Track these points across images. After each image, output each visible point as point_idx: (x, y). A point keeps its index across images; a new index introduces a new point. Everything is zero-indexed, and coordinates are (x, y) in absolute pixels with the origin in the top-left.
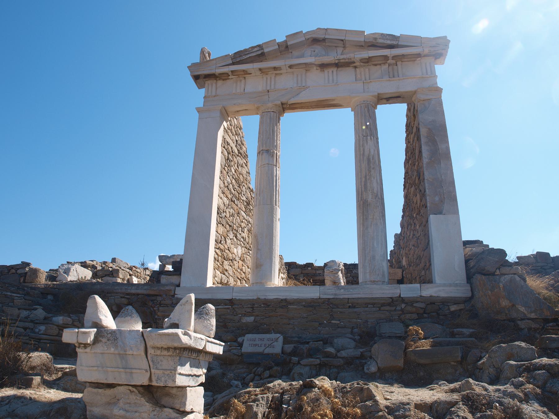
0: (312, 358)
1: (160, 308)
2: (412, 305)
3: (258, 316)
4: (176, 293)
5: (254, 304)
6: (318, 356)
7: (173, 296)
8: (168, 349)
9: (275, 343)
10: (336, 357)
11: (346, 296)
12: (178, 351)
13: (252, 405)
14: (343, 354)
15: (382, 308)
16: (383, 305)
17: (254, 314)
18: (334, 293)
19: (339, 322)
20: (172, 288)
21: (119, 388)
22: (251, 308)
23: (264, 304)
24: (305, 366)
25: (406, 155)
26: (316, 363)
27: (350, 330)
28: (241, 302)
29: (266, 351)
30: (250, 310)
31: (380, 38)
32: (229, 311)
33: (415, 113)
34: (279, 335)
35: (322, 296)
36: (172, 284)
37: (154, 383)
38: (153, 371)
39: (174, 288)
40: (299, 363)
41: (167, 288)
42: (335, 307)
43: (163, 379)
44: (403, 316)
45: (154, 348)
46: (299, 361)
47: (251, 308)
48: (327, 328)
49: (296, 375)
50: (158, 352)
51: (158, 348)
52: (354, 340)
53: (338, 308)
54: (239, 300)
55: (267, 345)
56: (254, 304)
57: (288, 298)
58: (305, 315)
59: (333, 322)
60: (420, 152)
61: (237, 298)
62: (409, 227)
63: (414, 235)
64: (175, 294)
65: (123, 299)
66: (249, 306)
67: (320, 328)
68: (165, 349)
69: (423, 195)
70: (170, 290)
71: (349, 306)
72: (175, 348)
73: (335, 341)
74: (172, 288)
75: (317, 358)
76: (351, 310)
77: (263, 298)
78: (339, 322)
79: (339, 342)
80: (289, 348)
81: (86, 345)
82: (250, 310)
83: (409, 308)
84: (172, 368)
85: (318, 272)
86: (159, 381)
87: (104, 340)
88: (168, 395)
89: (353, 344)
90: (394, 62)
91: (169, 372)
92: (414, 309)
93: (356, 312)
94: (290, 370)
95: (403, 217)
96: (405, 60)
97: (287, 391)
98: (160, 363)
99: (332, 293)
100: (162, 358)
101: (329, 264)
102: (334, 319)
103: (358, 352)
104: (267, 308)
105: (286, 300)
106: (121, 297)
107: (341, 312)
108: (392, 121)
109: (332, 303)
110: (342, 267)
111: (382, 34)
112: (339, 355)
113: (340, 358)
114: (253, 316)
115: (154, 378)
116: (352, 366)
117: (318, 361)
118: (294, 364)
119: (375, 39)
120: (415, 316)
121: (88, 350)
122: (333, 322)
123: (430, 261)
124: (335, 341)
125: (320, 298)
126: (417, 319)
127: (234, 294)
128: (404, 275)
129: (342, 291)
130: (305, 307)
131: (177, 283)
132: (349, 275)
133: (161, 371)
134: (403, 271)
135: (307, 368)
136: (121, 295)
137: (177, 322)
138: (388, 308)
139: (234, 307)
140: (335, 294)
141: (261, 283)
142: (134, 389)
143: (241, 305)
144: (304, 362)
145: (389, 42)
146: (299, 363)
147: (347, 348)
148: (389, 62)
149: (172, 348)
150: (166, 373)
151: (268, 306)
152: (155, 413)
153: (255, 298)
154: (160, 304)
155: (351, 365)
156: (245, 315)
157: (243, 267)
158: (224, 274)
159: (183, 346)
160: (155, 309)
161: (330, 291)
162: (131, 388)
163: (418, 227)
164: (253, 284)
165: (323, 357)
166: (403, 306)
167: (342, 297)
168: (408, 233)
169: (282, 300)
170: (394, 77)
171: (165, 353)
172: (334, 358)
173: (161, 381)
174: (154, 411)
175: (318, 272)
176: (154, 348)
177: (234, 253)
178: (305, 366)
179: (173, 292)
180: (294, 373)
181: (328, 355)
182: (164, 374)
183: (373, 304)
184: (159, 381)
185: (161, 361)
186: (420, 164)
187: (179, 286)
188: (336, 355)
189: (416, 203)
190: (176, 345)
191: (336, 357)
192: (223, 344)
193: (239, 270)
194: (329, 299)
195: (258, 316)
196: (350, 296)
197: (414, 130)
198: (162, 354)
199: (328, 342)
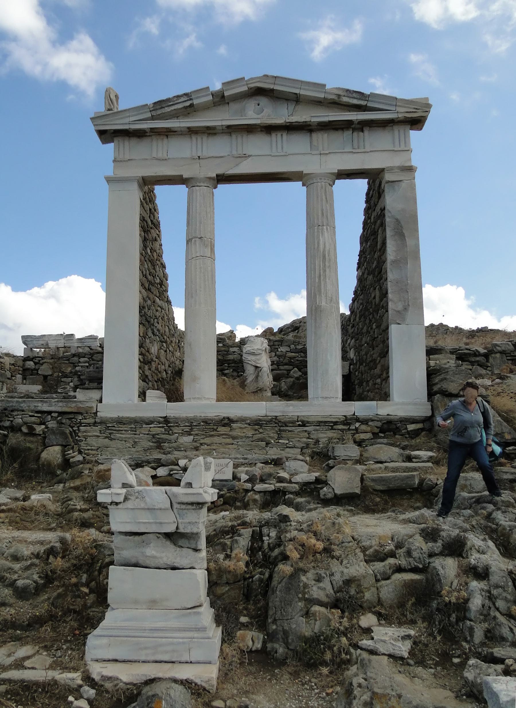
0: (266, 483)
1: (81, 428)
2: (367, 424)
6: (271, 482)
7: (96, 414)
9: (225, 469)
11: (297, 414)
14: (298, 478)
15: (335, 427)
16: (336, 423)
19: (288, 442)
21: (149, 535)
23: (203, 422)
25: (364, 228)
26: (271, 489)
30: (187, 429)
31: (344, 96)
33: (381, 191)
37: (181, 530)
38: (180, 521)
41: (88, 405)
44: (357, 435)
45: (179, 503)
46: (252, 487)
50: (183, 507)
51: (183, 503)
52: (306, 462)
53: (287, 426)
55: (217, 471)
59: (280, 441)
60: (384, 243)
62: (362, 319)
63: (368, 332)
64: (97, 412)
65: (33, 418)
66: (187, 424)
69: (384, 294)
75: (271, 484)
78: (288, 442)
81: (117, 504)
83: (364, 427)
85: (232, 350)
87: (132, 498)
89: (307, 467)
90: (359, 126)
92: (369, 429)
93: (306, 431)
95: (354, 300)
96: (374, 125)
103: (312, 477)
106: (31, 416)
107: (290, 431)
108: (351, 196)
111: (347, 90)
112: (293, 480)
113: (295, 483)
115: (180, 526)
119: (339, 96)
120: (369, 436)
121: (120, 506)
122: (280, 441)
123: (388, 373)
126: (372, 439)
127: (168, 411)
128: (351, 370)
129: (291, 408)
130: (249, 425)
131: (98, 397)
134: (350, 365)
136: (31, 414)
138: (341, 427)
140: (283, 412)
142: (160, 535)
143: (177, 423)
145: (355, 102)
148: (353, 126)
152: (177, 552)
154: (81, 423)
160: (74, 428)
162: (157, 535)
163: (374, 327)
166: (357, 425)
168: (360, 324)
170: (358, 148)
171: (190, 507)
174: (176, 551)
175: (232, 350)
176: (179, 503)
177: (152, 353)
181: (281, 480)
183: (326, 422)
186: (383, 258)
187: (101, 401)
188: (290, 480)
189: (375, 298)
191: (290, 482)
193: (156, 371)
194: (276, 417)
195: (197, 435)
197: (378, 209)
198: (187, 508)
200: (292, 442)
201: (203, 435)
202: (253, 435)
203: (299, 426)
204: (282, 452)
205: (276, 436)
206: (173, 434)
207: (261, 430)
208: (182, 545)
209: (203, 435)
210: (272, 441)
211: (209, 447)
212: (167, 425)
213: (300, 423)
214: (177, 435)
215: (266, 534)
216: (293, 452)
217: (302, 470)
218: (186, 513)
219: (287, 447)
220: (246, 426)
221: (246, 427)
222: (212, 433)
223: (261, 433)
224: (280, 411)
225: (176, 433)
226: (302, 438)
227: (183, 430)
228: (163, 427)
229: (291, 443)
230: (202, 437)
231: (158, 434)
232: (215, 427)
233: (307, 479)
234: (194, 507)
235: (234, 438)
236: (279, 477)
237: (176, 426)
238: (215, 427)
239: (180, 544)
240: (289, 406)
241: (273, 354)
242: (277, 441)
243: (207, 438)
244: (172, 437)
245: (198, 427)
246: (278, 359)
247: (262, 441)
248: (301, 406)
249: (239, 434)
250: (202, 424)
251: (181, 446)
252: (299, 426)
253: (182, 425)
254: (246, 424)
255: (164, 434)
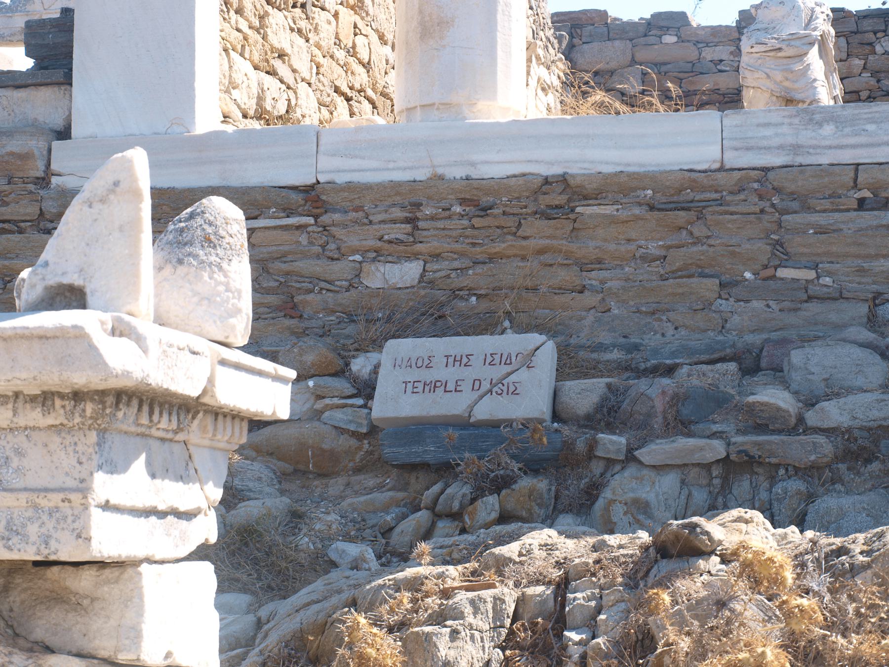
0: (690, 435)
3: (436, 256)
4: (54, 166)
5: (418, 205)
6: (716, 428)
7: (43, 181)
8: (45, 399)
9: (523, 375)
10: (800, 427)
11: (847, 156)
12: (89, 408)
13: (428, 636)
14: (834, 413)
17: (419, 247)
18: (790, 140)
19: (812, 275)
20: (36, 145)
22: (407, 221)
23: (463, 202)
24: (659, 469)
26: (709, 457)
27: (864, 309)
28: (359, 199)
29: (485, 411)
30: (399, 231)
32: (303, 239)
34: (536, 338)
35: (735, 159)
36: (35, 128)
39: (43, 144)
40: (630, 458)
42: (795, 205)
43: (33, 530)
47: (407, 221)
48: (756, 304)
49: (618, 513)
53: (807, 208)
54: (350, 187)
56: (418, 205)
57: (574, 170)
58: (653, 248)
61: (341, 179)
66: (397, 213)
67: (723, 305)
68: (33, 399)
70: (26, 157)
71: (861, 202)
72: (78, 396)
73: (797, 357)
74: (36, 145)
75: (713, 435)
76: (868, 218)
77: (459, 172)
79: (812, 361)
80: (585, 394)
82: (399, 231)
84: (71, 483)
85: (709, 54)
86: (15, 540)
88: (60, 598)
91: (55, 499)
94: (592, 492)
97: (585, 572)
98: (15, 462)
99: (776, 142)
100: (20, 439)
101: (761, 15)
102: (786, 258)
104: (477, 222)
105: (563, 180)
107: (821, 231)
109: (777, 190)
110: (824, 26)
112: (812, 418)
114: (415, 256)
116: (875, 466)
117: (717, 449)
118: (610, 462)
122: (782, 273)
124: (797, 357)
125: (721, 169)
127: (325, 163)
129: (828, 129)
130: (652, 208)
131: (58, 122)
132: (858, 63)
133: (23, 496)
135: (669, 482)
137: (77, 281)
139: (325, 219)
140: (796, 148)
141: (447, 105)
143: (357, 209)
144: (654, 451)
146: (630, 458)
147: (850, 391)
149: (62, 396)
150: (43, 502)
151: (485, 210)
153: (422, 175)
155: (868, 461)
156: (378, 255)
157: (360, 40)
158: (272, 73)
159: (113, 384)
161: (768, 132)
164: (409, 110)
165: (739, 432)
167: (825, 160)
169: (547, 181)
171: (34, 416)
172: (792, 431)
173: (25, 538)
178: (659, 469)
179: (41, 165)
180: (611, 502)
181: (762, 422)
182: (36, 507)
184: (15, 540)
185: (19, 453)
187: (64, 134)
188: (801, 420)
190: (80, 379)
191: (800, 427)
192: (292, 374)
193: (340, 55)
194: (765, 170)
195: (436, 256)
196: (863, 156)
198: (21, 421)
199: (764, 363)
200: (829, 274)
201: (462, 254)
202: (668, 248)
203: (862, 204)
204: (791, 319)
205: (761, 250)
206: (341, 255)
207: (699, 230)
208: (51, 641)
209: (462, 254)
210: (748, 275)
211: (485, 305)
212: (316, 217)
213: (866, 194)
214: (358, 257)
215: (578, 617)
216: (833, 317)
217: (860, 382)
218: (19, 453)
219: (810, 298)
220: (637, 211)
221: (637, 218)
222: (499, 247)
223: (698, 241)
224: (781, 147)
225: (355, 251)
226: (877, 256)
227: (381, 239)
228: (300, 227)
229: (827, 280)
230: (456, 264)
231: (282, 257)
232: (511, 222)
233: (875, 414)
234: (56, 418)
235: (584, 266)
236: (751, 408)
237: (356, 222)
238: (511, 222)
239: (39, 633)
240: (820, 124)
241: (858, 63)
242: (769, 272)
243: (479, 269)
244: (337, 266)
245: (440, 224)
246: (873, 82)
247: (703, 275)
248: (872, 121)
249: (612, 247)
250: (458, 209)
251: (375, 302)
252: (862, 204)
253: (380, 217)
254: (640, 204)
255: (305, 256)
